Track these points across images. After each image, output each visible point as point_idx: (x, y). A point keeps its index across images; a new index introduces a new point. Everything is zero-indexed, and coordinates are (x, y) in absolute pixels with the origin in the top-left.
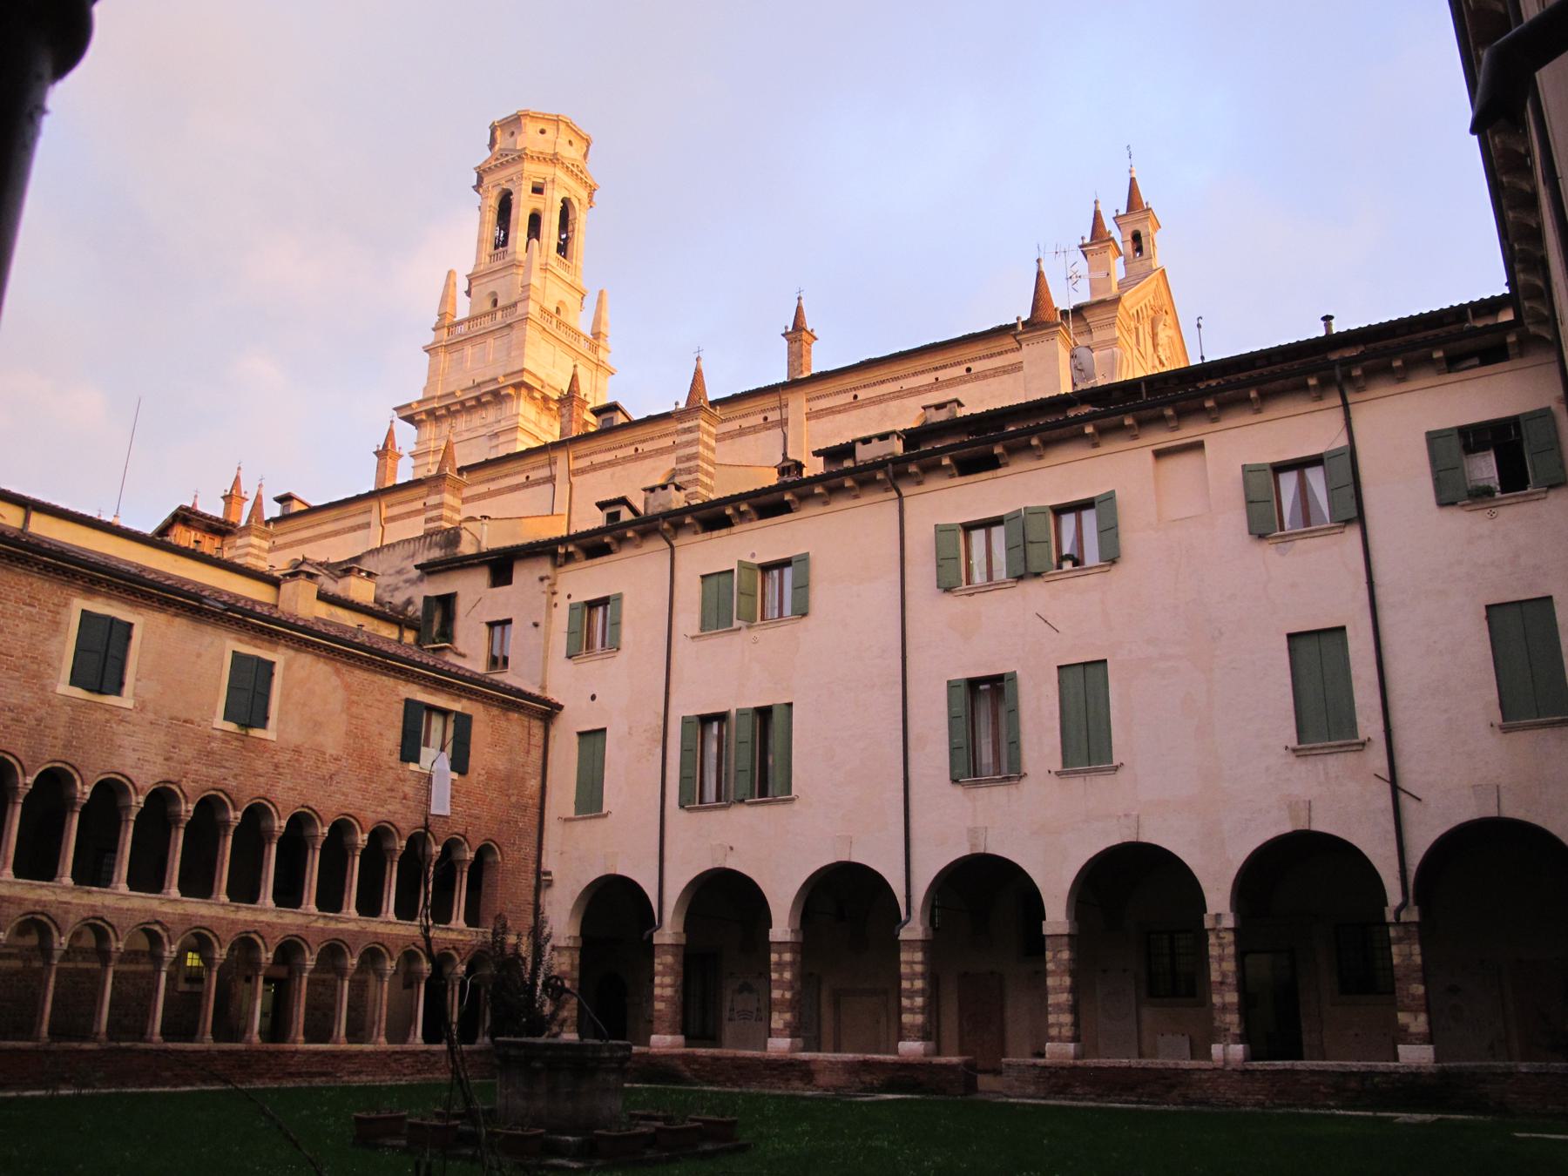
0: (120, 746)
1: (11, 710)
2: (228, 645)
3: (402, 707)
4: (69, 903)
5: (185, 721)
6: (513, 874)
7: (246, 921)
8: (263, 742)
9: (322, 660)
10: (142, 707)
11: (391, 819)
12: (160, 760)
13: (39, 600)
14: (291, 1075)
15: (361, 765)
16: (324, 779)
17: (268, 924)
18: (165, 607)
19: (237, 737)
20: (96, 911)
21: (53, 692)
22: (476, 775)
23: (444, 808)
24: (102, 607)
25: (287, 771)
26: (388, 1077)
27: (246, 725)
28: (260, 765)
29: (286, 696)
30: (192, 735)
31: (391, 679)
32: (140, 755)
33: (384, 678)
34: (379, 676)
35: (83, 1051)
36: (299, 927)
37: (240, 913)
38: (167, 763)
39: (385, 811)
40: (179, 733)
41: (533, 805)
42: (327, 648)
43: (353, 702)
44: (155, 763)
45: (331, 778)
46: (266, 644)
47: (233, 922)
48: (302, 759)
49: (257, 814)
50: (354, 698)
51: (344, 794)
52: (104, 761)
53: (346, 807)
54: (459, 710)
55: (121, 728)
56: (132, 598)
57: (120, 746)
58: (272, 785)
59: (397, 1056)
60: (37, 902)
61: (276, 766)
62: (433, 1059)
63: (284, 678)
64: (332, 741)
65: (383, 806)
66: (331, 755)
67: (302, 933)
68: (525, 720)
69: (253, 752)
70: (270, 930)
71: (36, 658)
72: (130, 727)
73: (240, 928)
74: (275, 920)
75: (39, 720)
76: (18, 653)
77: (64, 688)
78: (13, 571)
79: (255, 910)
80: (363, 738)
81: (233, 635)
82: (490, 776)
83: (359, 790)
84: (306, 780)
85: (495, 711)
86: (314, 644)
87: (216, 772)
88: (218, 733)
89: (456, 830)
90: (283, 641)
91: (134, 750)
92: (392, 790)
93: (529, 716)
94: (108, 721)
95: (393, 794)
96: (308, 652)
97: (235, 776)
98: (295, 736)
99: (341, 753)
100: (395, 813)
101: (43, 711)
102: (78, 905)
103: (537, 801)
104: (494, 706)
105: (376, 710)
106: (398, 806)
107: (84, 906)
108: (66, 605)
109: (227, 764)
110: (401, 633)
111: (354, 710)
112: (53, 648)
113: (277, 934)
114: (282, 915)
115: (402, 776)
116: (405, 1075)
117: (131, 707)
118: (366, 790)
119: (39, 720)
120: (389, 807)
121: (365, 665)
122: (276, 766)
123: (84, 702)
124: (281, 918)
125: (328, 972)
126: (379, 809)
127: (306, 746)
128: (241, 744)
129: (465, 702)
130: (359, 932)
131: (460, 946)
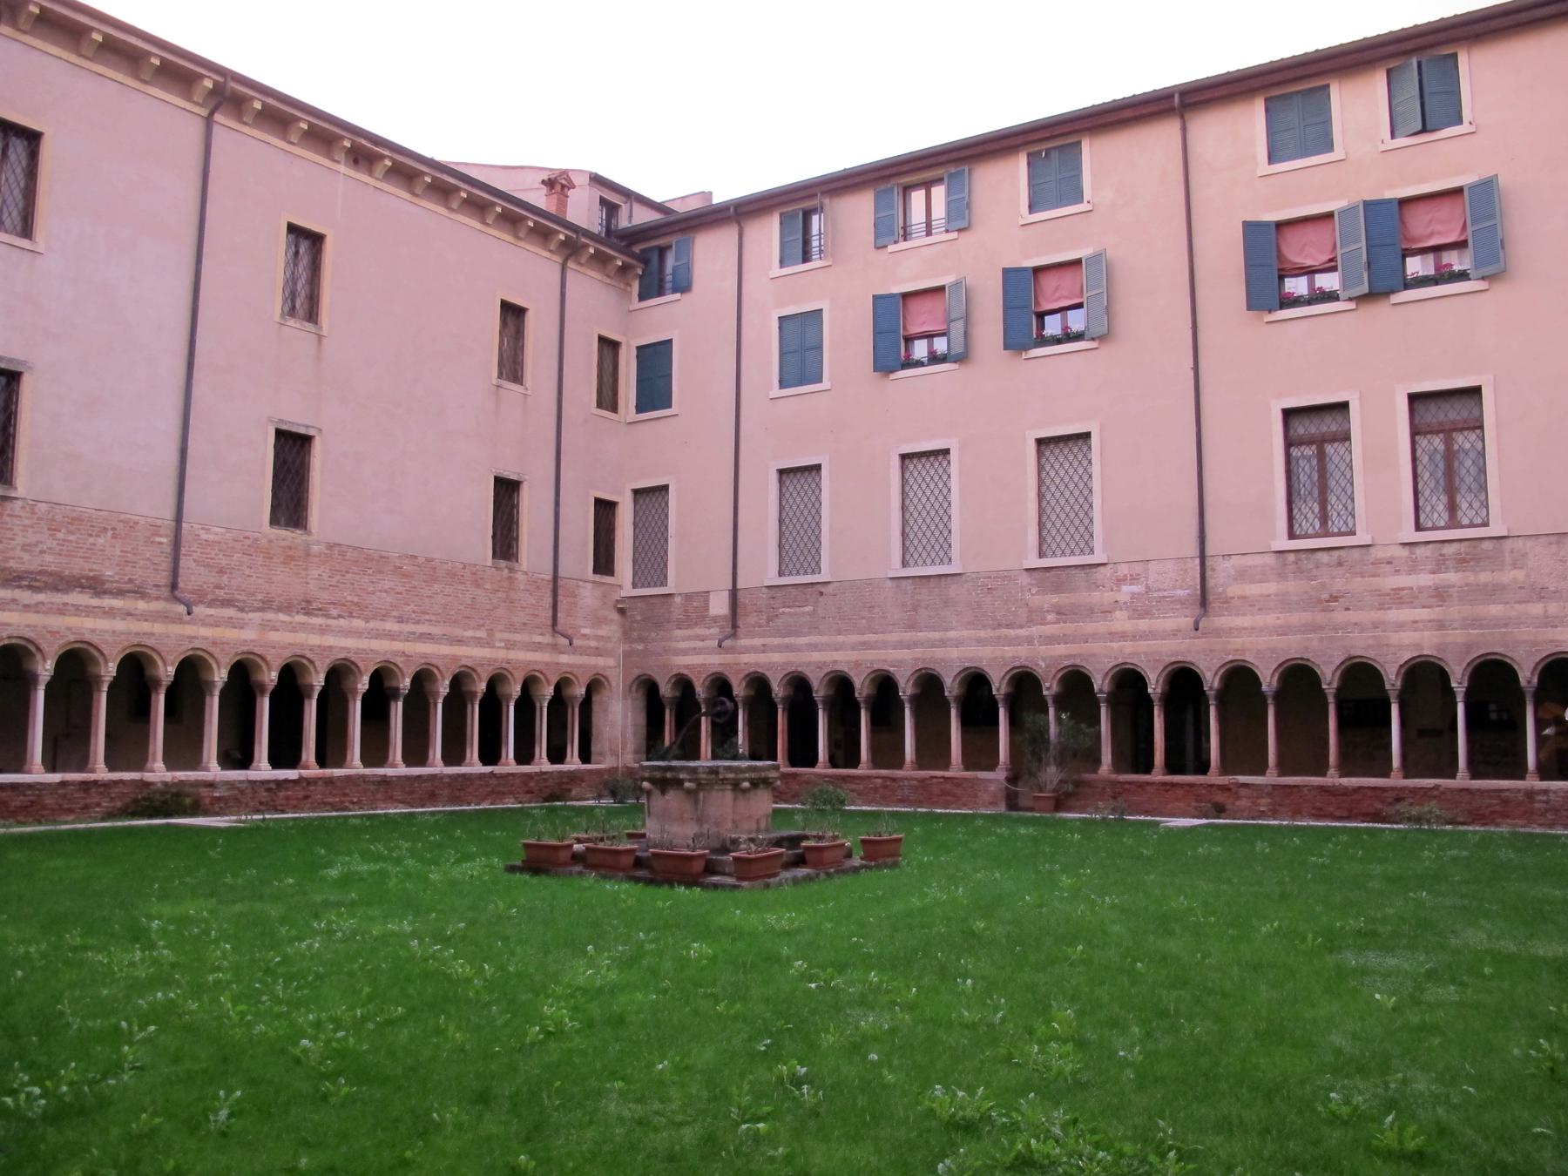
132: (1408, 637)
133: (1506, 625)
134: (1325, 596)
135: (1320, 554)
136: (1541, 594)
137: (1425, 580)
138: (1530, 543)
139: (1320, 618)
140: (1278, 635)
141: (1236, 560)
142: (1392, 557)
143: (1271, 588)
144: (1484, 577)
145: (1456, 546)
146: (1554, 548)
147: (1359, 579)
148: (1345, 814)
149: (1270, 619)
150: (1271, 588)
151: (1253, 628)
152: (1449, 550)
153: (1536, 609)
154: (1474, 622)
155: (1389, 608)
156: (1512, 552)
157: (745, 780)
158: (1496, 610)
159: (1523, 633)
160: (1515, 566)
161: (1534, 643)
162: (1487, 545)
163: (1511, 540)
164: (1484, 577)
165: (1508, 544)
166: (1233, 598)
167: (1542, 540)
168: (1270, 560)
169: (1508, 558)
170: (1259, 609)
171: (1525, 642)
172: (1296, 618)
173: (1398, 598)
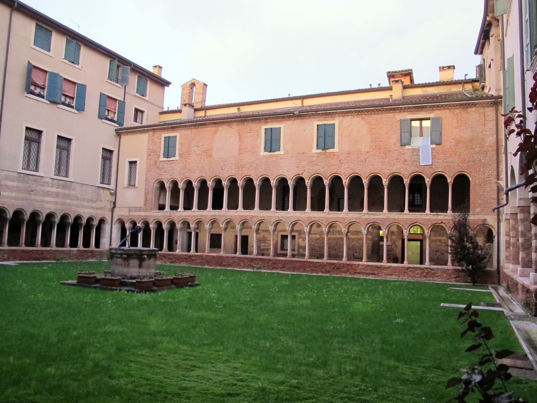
0: (281, 167)
1: (249, 164)
2: (315, 123)
3: (399, 123)
5: (303, 153)
6: (480, 185)
7: (332, 218)
8: (333, 153)
9: (355, 116)
10: (287, 152)
11: (398, 171)
14: (358, 273)
15: (379, 152)
16: (362, 161)
17: (342, 218)
18: (290, 119)
19: (324, 154)
20: (279, 218)
21: (260, 155)
22: (448, 143)
23: (423, 162)
24: (270, 126)
25: (345, 161)
26: (406, 278)
27: (325, 149)
29: (340, 135)
30: (306, 157)
31: (391, 114)
33: (388, 114)
34: (384, 115)
36: (357, 218)
37: (330, 215)
39: (395, 168)
41: (492, 150)
42: (355, 112)
43: (373, 128)
44: (293, 169)
45: (365, 160)
47: (327, 218)
49: (249, 181)
50: (373, 127)
53: (374, 170)
54: (434, 116)
55: (281, 161)
56: (279, 120)
57: (281, 167)
58: (339, 168)
59: (411, 269)
60: (262, 217)
61: (340, 161)
62: (433, 272)
63: (339, 128)
64: (364, 146)
65: (393, 167)
66: (365, 152)
68: (481, 110)
69: (329, 158)
70: (343, 220)
74: (345, 217)
77: (262, 153)
79: (402, 214)
80: (380, 141)
81: (316, 120)
82: (458, 142)
83: (380, 162)
85: (457, 111)
86: (349, 112)
88: (315, 154)
89: (438, 170)
90: (337, 115)
91: (286, 167)
93: (484, 107)
94: (277, 160)
95: (398, 161)
97: (323, 168)
99: (369, 150)
100: (400, 168)
103: (495, 148)
104: (457, 108)
105: (384, 129)
107: (275, 217)
108: (260, 129)
109: (319, 164)
110: (463, 87)
111: (374, 131)
112: (258, 143)
114: (348, 214)
115: (402, 152)
116: (416, 277)
118: (384, 162)
120: (397, 166)
121: (376, 112)
122: (340, 161)
124: (347, 215)
125: (443, 236)
127: (352, 150)
128: (325, 156)
129: (437, 112)
131: (446, 222)
132: (49, 206)
134: (30, 190)
135: (30, 176)
136: (77, 199)
137: (54, 190)
139: (28, 196)
140: (15, 200)
141: (5, 172)
142: (48, 182)
143: (15, 184)
144: (67, 192)
145: (62, 181)
147: (39, 186)
148: (28, 258)
149: (14, 194)
150: (15, 184)
151: (8, 197)
152: (61, 182)
153: (76, 202)
154: (64, 204)
155: (46, 197)
157: (145, 254)
158: (68, 201)
159: (73, 208)
163: (73, 183)
164: (67, 192)
165: (73, 184)
166: (3, 185)
167: (79, 184)
168: (16, 175)
169: (72, 188)
170: (11, 191)
172: (21, 195)
173: (48, 194)
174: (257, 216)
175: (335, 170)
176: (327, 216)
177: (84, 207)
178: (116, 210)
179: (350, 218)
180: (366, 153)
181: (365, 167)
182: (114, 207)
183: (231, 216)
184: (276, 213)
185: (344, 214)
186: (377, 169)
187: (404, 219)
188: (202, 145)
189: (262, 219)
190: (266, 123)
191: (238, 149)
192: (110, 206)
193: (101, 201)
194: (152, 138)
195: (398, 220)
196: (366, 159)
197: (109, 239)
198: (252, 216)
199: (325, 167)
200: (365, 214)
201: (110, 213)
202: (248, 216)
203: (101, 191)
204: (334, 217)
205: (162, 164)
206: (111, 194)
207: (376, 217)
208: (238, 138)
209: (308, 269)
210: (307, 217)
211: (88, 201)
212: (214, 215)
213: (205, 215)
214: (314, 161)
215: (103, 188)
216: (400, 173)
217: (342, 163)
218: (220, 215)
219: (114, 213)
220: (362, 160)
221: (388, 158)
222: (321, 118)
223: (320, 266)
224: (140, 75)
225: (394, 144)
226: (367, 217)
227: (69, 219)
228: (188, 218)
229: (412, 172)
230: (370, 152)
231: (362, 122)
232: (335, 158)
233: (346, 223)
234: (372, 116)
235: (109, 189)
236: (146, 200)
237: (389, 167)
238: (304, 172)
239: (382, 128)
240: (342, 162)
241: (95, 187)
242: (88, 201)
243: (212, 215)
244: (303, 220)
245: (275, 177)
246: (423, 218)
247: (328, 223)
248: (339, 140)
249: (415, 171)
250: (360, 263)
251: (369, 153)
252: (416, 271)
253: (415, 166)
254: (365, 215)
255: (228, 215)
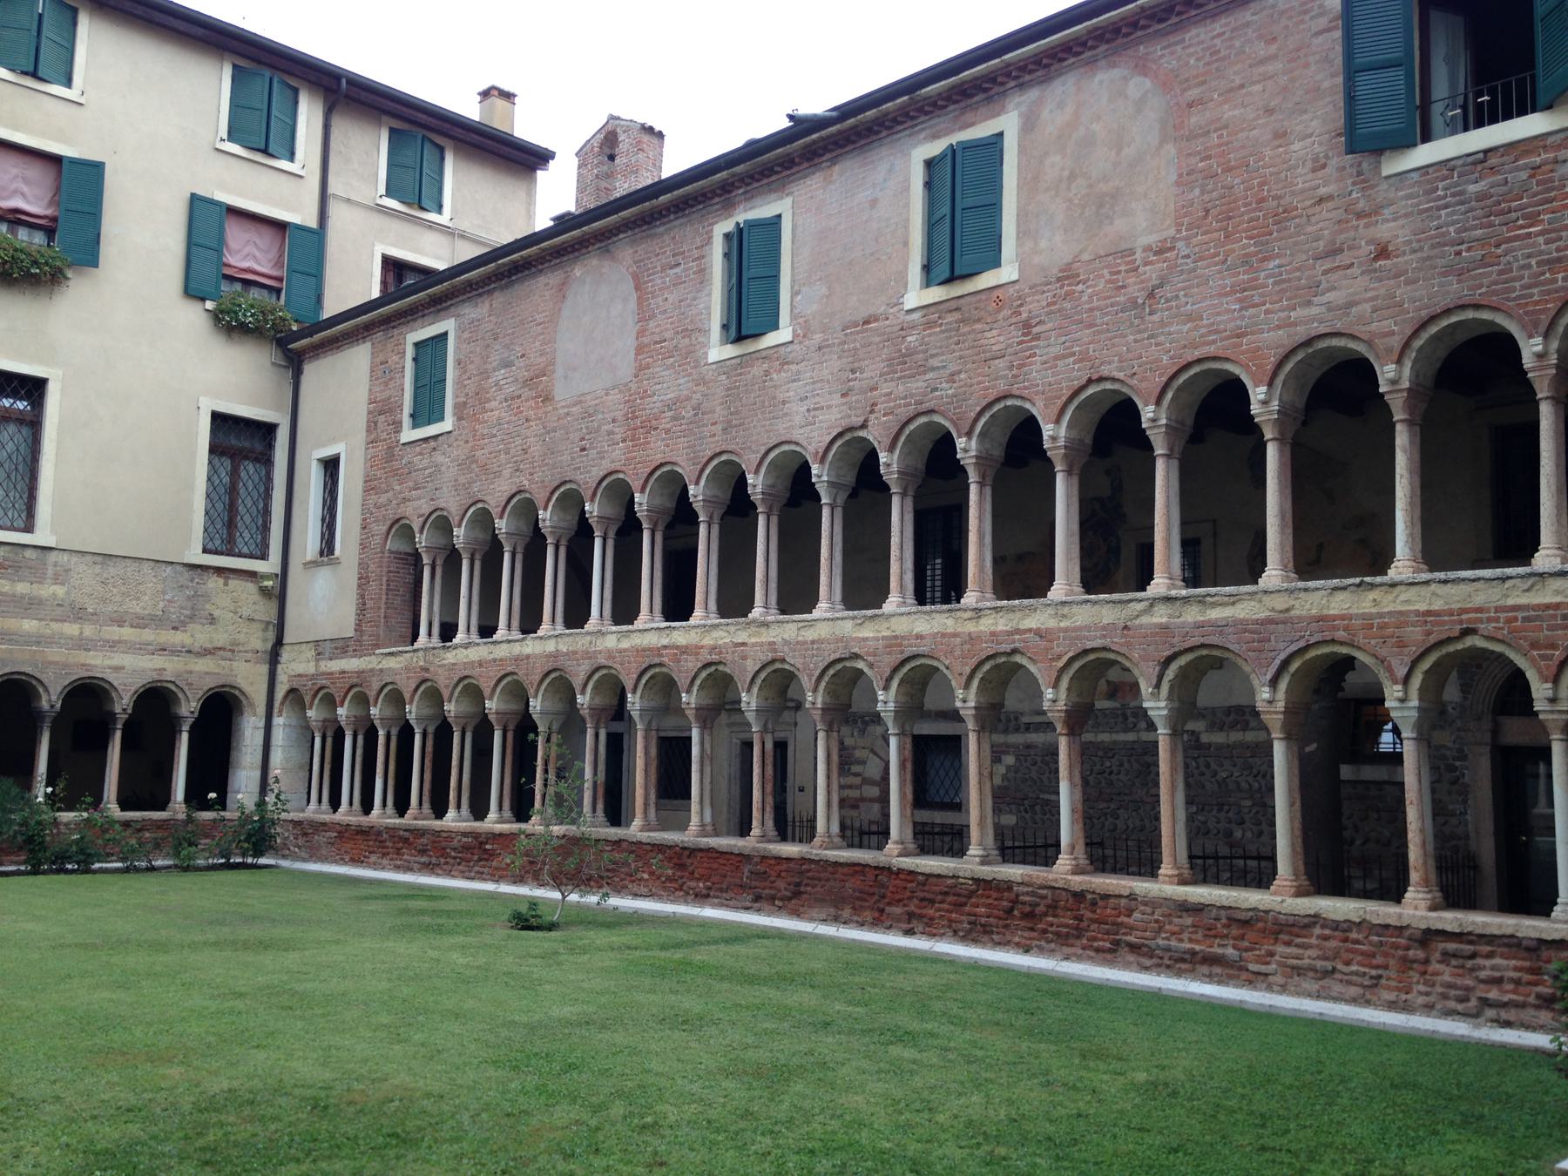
0: (784, 402)
4: (744, 644)
5: (866, 322)
7: (993, 634)
11: (1339, 326)
12: (837, 399)
13: (683, 253)
17: (1038, 633)
20: (775, 651)
25: (1049, 326)
28: (995, 339)
29: (1029, 184)
30: (877, 339)
32: (809, 403)
35: (779, 859)
36: (1108, 629)
37: (983, 621)
38: (848, 399)
39: (1314, 310)
40: (858, 345)
44: (829, 407)
45: (1151, 295)
46: (983, 111)
47: (971, 639)
48: (1080, 287)
50: (1194, 93)
51: (1190, 318)
52: (767, 431)
57: (784, 402)
58: (1020, 366)
59: (1452, 946)
60: (713, 648)
61: (1027, 326)
65: (1309, 303)
66: (1148, 249)
67: (1116, 641)
69: (979, 320)
71: (687, 330)
72: (794, 367)
73: (987, 649)
74: (1052, 623)
75: (697, 408)
76: (667, 335)
78: (655, 235)
83: (1233, 292)
84: (1091, 326)
87: (918, 385)
88: (916, 316)
92: (1334, 252)
94: (767, 373)
95: (1339, 260)
96: (1072, 67)
98: (1056, 248)
99: (1172, 232)
101: (698, 396)
102: (754, 645)
105: (1258, 88)
106: (1363, 281)
107: (762, 645)
109: (935, 362)
111: (1195, 120)
113: (1058, 650)
114: (1066, 610)
117: (789, 338)
119: (697, 408)
120: (1330, 296)
122: (1027, 326)
123: (738, 361)
124: (1064, 616)
126: (1300, 313)
127: (1086, 257)
128: (956, 316)
130: (1269, 621)
133: (38, 643)
136: (78, 614)
138: (75, 559)
144: (22, 588)
146: (98, 569)
153: (71, 629)
156: (55, 566)
158: (29, 625)
159: (55, 654)
160: (57, 580)
161: (66, 665)
162: (29, 553)
163: (56, 552)
164: (22, 588)
165: (53, 556)
167: (88, 558)
169: (50, 572)
171: (56, 663)
174: (697, 647)
175: (1006, 376)
176: (970, 627)
177: (113, 645)
178: (286, 655)
179: (1076, 629)
180: (1160, 252)
181: (1150, 337)
182: (279, 643)
183: (610, 654)
184: (763, 630)
185: (1050, 611)
186: (1217, 332)
187: (1381, 615)
188: (523, 356)
189: (715, 657)
190: (729, 207)
191: (632, 353)
192: (259, 641)
193: (212, 620)
194: (381, 358)
195: (1346, 629)
196: (1155, 287)
197: (257, 774)
198: (677, 647)
199: (960, 372)
200: (1154, 601)
201: (265, 668)
202: (665, 647)
203: (214, 583)
204: (1000, 628)
205: (410, 455)
206: (264, 592)
207: (1215, 614)
208: (634, 297)
209: (897, 910)
210: (884, 638)
211: (140, 622)
212: (556, 655)
213: (528, 657)
214: (911, 353)
215: (219, 571)
216: (1353, 337)
217: (1037, 337)
218: (575, 653)
219: (280, 667)
220: (1134, 302)
221: (1278, 256)
222: (940, 122)
223: (946, 893)
224: (396, 124)
225: (1309, 165)
226: (1164, 620)
227: (39, 697)
228: (476, 672)
229: (1424, 314)
230: (1180, 244)
231: (1138, 85)
232: (1000, 316)
233: (1059, 657)
234: (1187, 36)
235: (252, 575)
236: (362, 609)
237: (1282, 310)
238: (872, 412)
239: (1242, 86)
240: (1035, 330)
241: (178, 568)
242: (140, 622)
243: (550, 655)
244: (868, 654)
245: (759, 456)
246: (1510, 602)
247: (975, 661)
248: (1022, 216)
249: (1448, 302)
250: (1141, 886)
251: (1172, 249)
252: (1488, 963)
253: (1444, 274)
254: (1152, 605)
255: (600, 652)
